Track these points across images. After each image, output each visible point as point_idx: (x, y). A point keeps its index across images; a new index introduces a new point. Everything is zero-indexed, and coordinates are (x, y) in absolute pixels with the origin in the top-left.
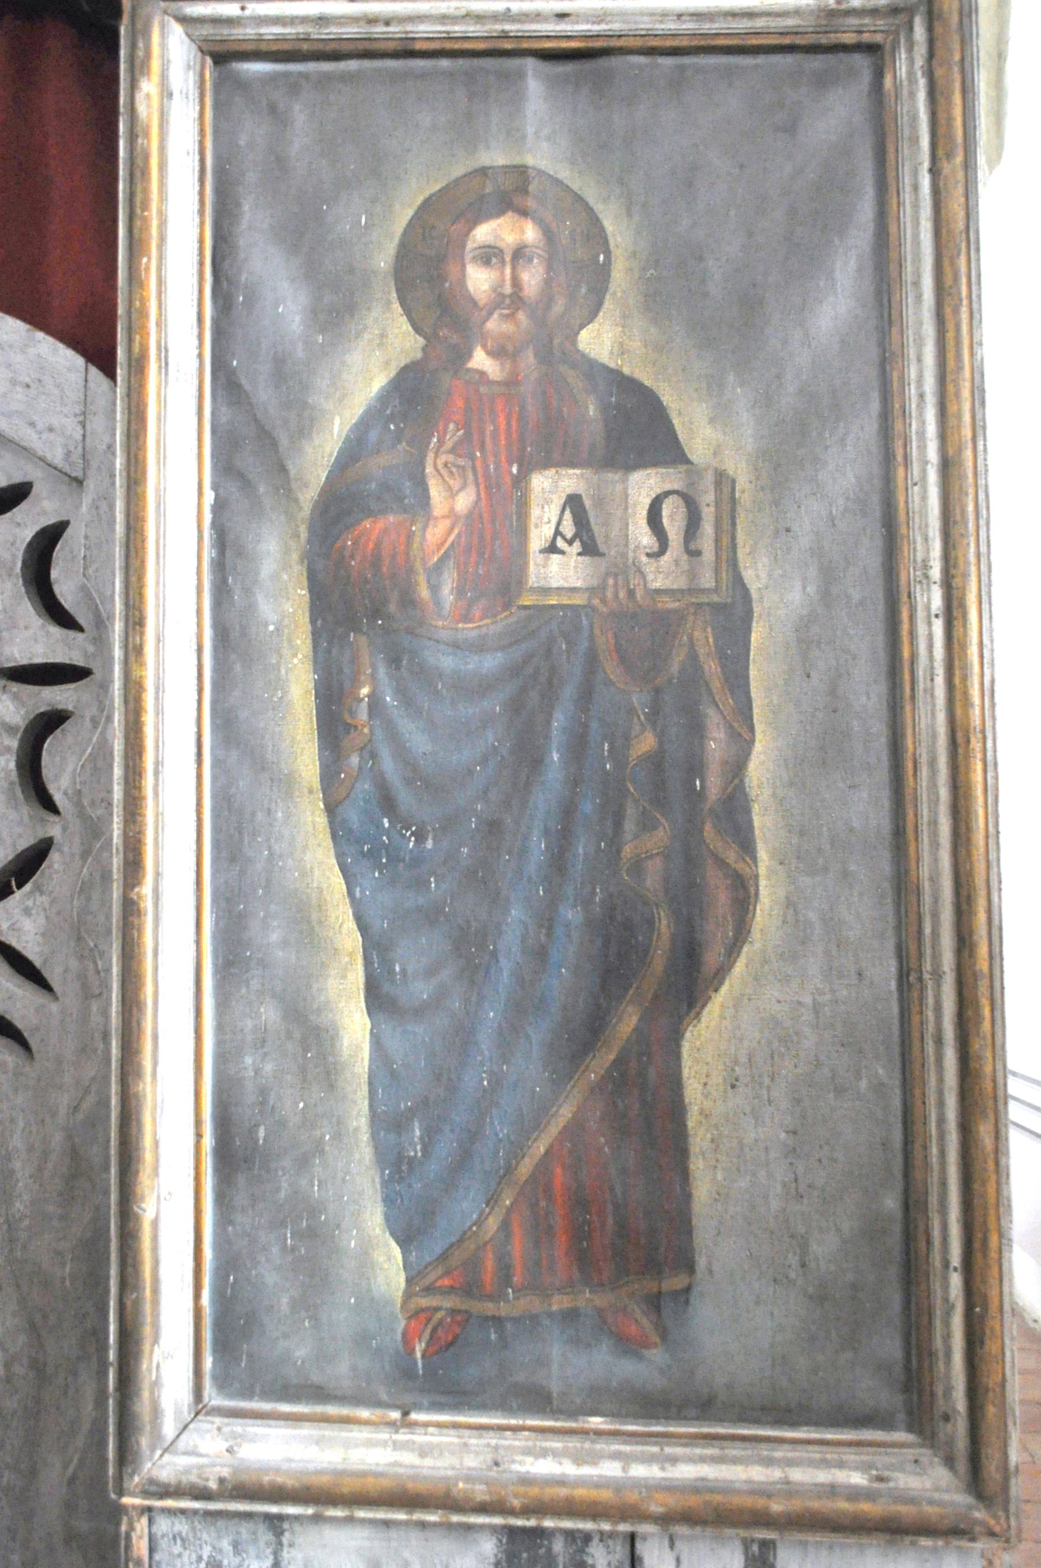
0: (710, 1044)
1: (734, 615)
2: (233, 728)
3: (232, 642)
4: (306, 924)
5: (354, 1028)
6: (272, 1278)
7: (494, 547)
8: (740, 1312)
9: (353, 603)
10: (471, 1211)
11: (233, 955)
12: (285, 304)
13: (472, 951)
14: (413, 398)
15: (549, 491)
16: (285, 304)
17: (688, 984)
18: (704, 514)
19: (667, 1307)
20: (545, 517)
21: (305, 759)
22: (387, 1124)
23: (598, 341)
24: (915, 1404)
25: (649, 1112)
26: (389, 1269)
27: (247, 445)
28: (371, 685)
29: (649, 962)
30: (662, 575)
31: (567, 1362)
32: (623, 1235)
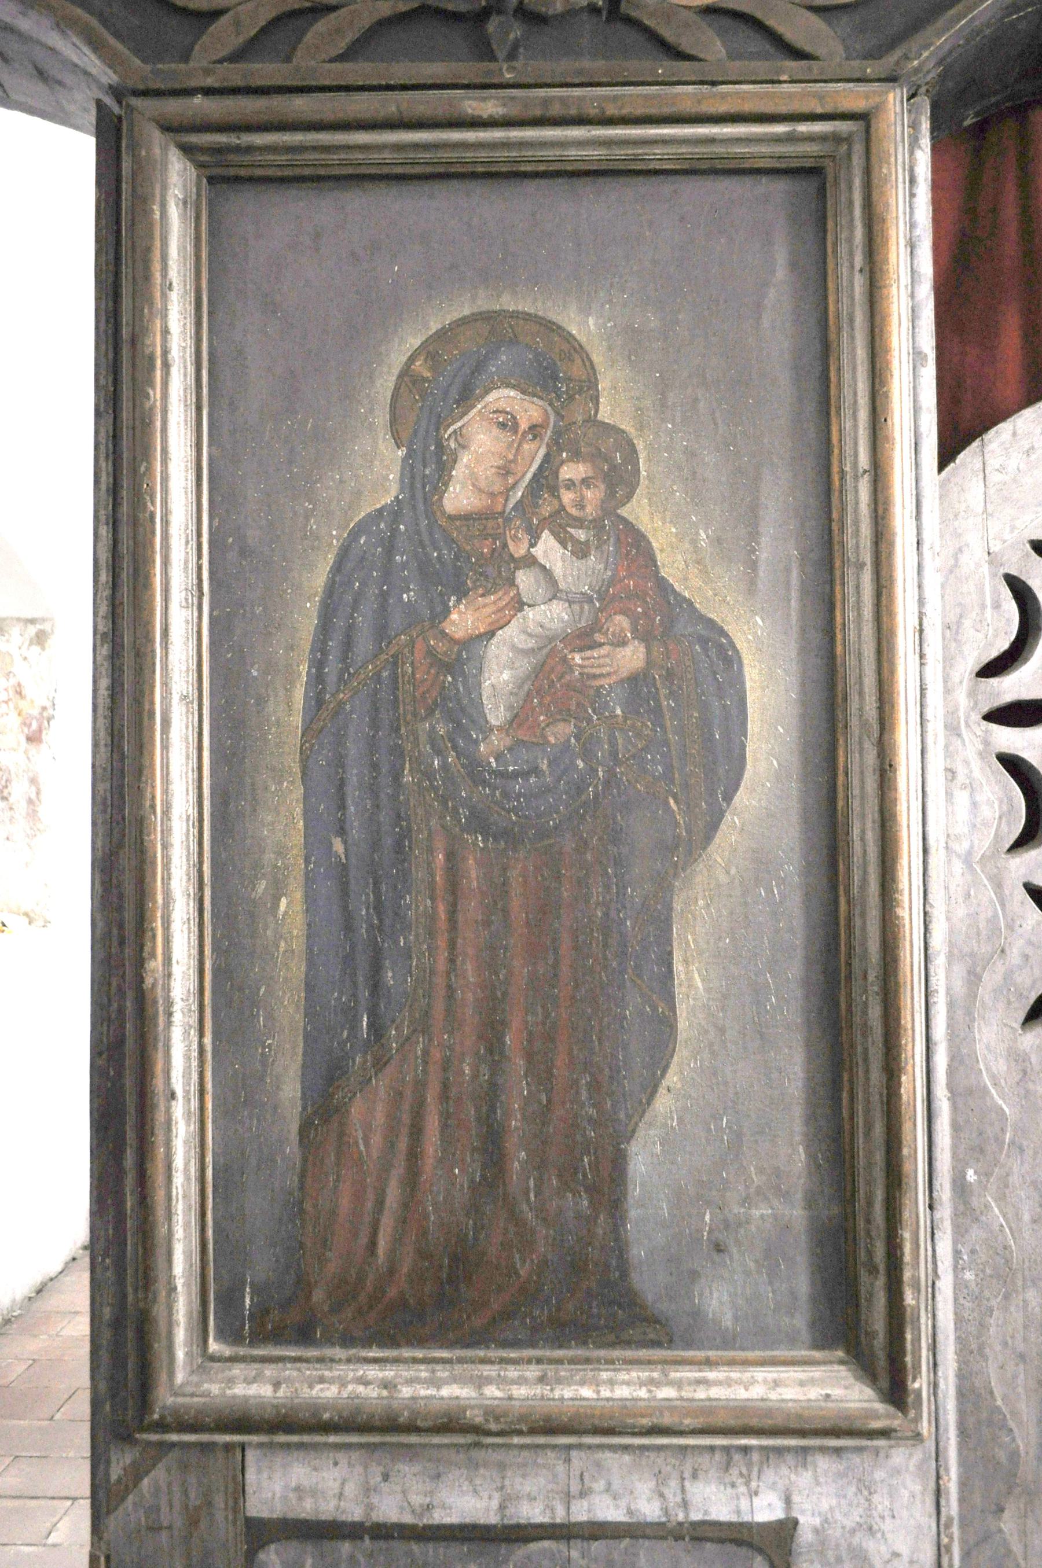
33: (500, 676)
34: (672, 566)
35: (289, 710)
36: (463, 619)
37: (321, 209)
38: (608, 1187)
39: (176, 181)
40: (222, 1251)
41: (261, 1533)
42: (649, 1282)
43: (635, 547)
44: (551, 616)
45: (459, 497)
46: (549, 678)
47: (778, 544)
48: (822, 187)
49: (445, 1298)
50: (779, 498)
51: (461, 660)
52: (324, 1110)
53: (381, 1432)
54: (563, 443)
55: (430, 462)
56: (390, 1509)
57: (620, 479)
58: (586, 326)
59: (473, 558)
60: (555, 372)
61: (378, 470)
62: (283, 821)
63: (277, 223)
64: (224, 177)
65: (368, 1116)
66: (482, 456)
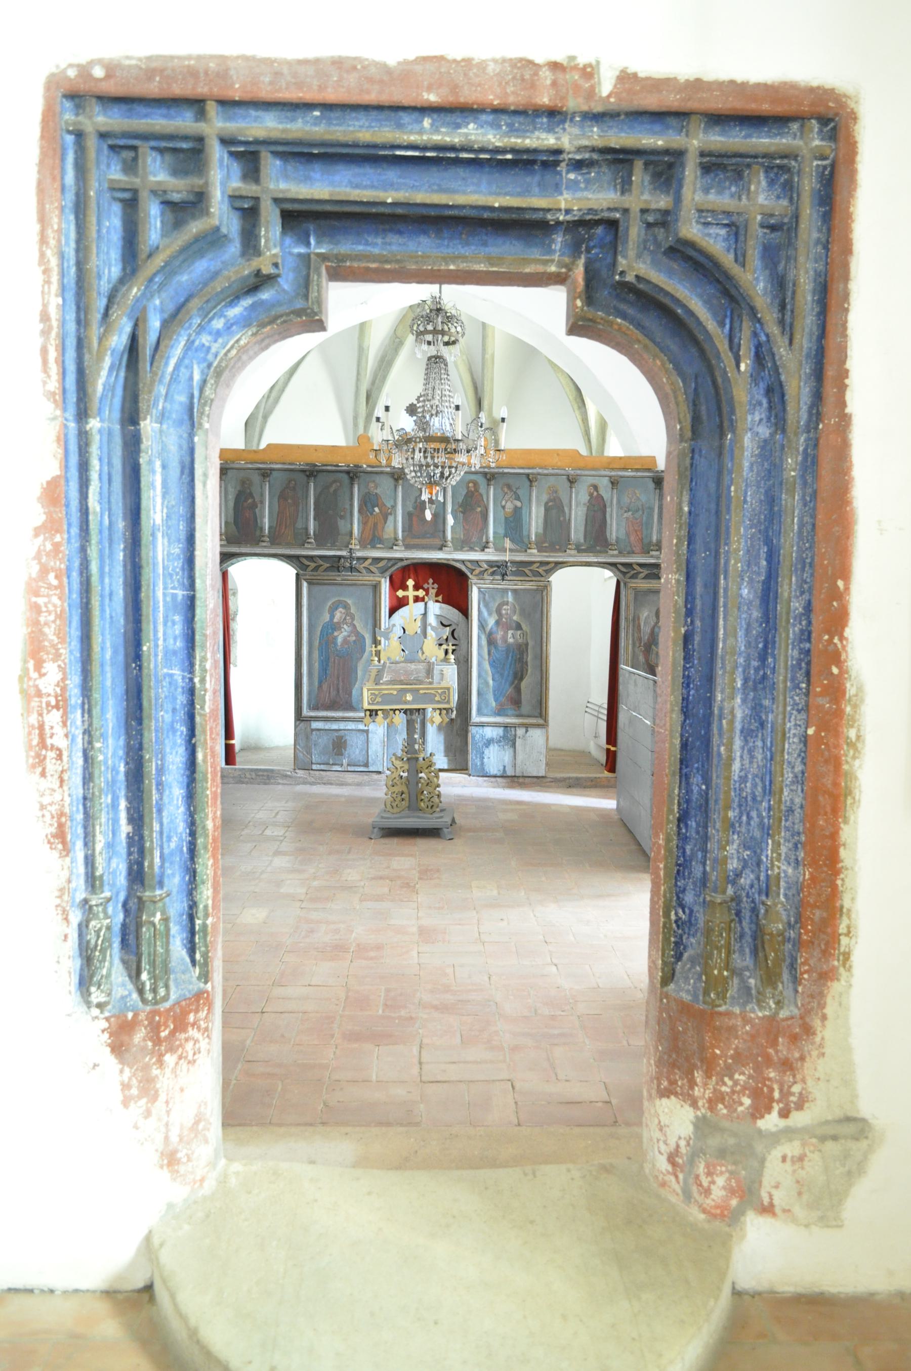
0: (523, 684)
1: (527, 645)
2: (479, 654)
3: (479, 645)
4: (486, 672)
5: (491, 682)
6: (483, 706)
7: (505, 639)
8: (526, 708)
9: (491, 642)
10: (503, 699)
11: (480, 676)
12: (485, 614)
13: (502, 675)
14: (497, 623)
15: (510, 633)
16: (485, 614)
17: (521, 679)
18: (524, 634)
19: (519, 707)
20: (510, 635)
21: (486, 657)
22: (494, 691)
23: (515, 618)
24: (541, 716)
25: (518, 690)
26: (494, 704)
27: (482, 626)
28: (493, 650)
29: (519, 676)
30: (520, 641)
31: (510, 712)
32: (516, 702)
33: (340, 640)
34: (359, 629)
35: (317, 643)
36: (336, 634)
37: (321, 587)
38: (350, 694)
39: (305, 584)
40: (309, 700)
41: (313, 730)
42: (354, 704)
43: (354, 626)
44: (345, 634)
45: (335, 620)
46: (345, 641)
47: (370, 626)
48: (376, 587)
49: (332, 706)
50: (370, 622)
51: (335, 638)
52: (320, 686)
53: (326, 719)
54: (347, 615)
55: (332, 616)
56: (327, 727)
57: (353, 619)
58: (349, 602)
59: (336, 627)
60: (346, 606)
61: (326, 617)
62: (316, 654)
63: (316, 589)
64: (310, 583)
65: (325, 687)
66: (338, 615)
